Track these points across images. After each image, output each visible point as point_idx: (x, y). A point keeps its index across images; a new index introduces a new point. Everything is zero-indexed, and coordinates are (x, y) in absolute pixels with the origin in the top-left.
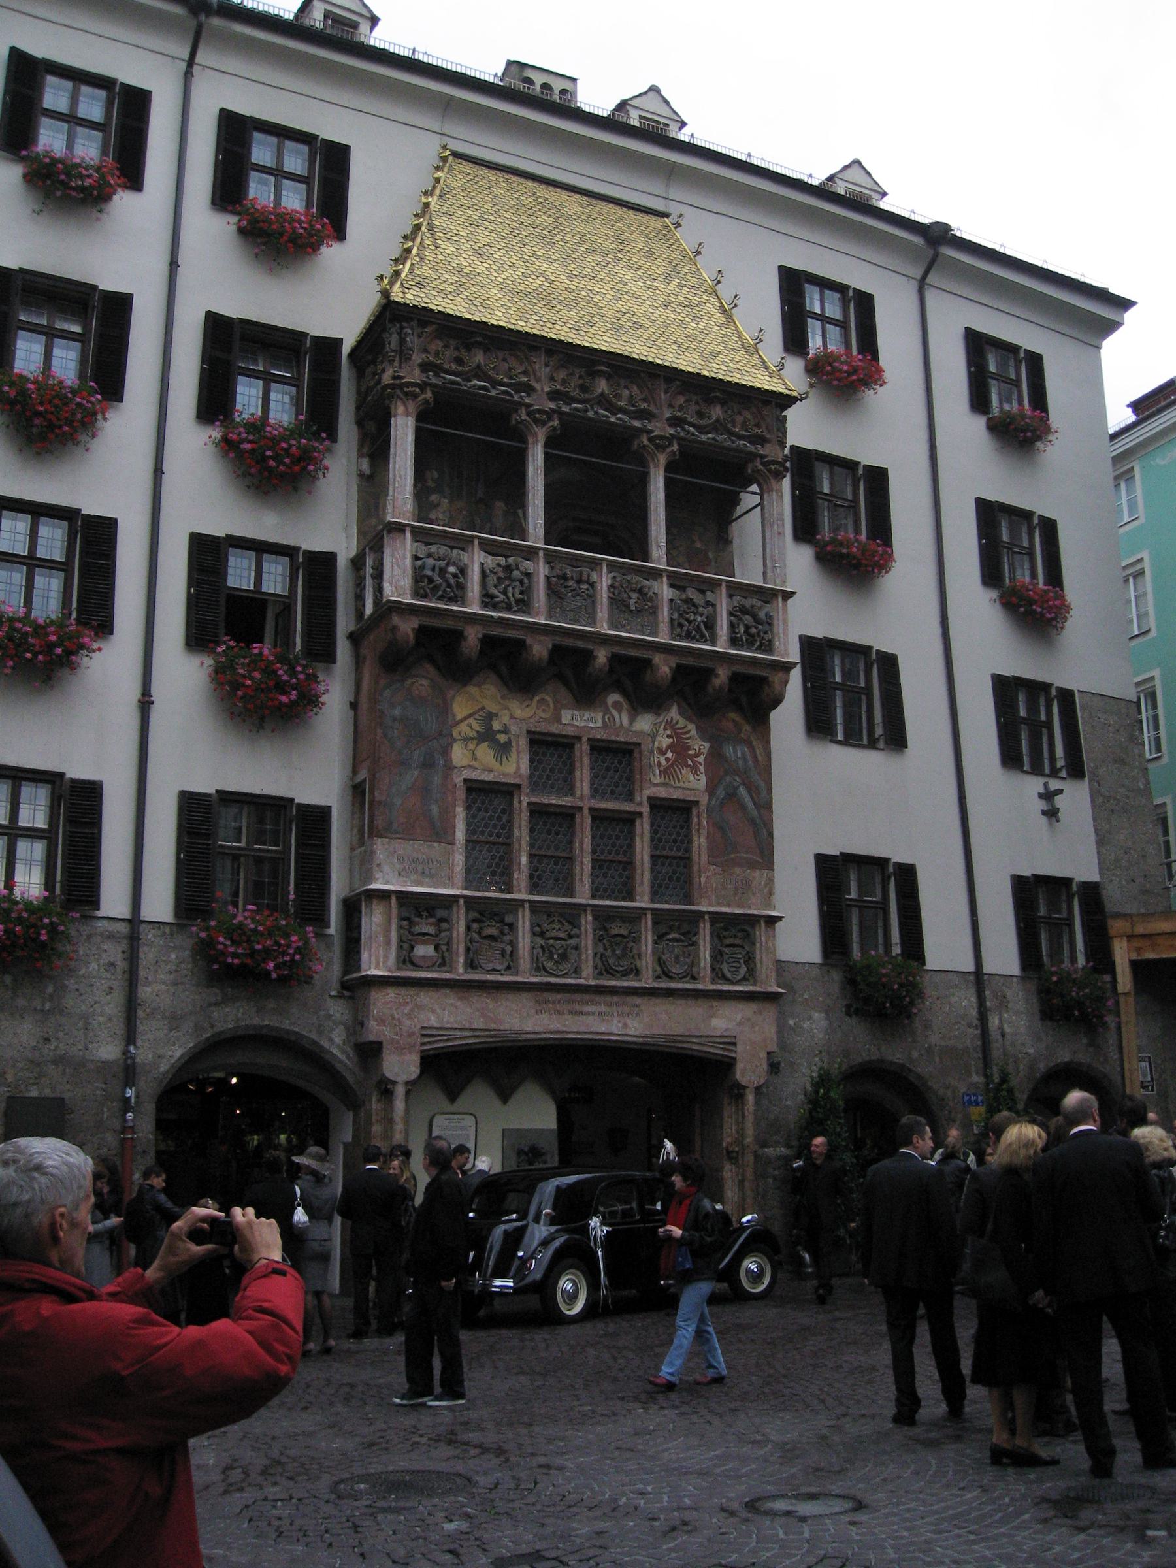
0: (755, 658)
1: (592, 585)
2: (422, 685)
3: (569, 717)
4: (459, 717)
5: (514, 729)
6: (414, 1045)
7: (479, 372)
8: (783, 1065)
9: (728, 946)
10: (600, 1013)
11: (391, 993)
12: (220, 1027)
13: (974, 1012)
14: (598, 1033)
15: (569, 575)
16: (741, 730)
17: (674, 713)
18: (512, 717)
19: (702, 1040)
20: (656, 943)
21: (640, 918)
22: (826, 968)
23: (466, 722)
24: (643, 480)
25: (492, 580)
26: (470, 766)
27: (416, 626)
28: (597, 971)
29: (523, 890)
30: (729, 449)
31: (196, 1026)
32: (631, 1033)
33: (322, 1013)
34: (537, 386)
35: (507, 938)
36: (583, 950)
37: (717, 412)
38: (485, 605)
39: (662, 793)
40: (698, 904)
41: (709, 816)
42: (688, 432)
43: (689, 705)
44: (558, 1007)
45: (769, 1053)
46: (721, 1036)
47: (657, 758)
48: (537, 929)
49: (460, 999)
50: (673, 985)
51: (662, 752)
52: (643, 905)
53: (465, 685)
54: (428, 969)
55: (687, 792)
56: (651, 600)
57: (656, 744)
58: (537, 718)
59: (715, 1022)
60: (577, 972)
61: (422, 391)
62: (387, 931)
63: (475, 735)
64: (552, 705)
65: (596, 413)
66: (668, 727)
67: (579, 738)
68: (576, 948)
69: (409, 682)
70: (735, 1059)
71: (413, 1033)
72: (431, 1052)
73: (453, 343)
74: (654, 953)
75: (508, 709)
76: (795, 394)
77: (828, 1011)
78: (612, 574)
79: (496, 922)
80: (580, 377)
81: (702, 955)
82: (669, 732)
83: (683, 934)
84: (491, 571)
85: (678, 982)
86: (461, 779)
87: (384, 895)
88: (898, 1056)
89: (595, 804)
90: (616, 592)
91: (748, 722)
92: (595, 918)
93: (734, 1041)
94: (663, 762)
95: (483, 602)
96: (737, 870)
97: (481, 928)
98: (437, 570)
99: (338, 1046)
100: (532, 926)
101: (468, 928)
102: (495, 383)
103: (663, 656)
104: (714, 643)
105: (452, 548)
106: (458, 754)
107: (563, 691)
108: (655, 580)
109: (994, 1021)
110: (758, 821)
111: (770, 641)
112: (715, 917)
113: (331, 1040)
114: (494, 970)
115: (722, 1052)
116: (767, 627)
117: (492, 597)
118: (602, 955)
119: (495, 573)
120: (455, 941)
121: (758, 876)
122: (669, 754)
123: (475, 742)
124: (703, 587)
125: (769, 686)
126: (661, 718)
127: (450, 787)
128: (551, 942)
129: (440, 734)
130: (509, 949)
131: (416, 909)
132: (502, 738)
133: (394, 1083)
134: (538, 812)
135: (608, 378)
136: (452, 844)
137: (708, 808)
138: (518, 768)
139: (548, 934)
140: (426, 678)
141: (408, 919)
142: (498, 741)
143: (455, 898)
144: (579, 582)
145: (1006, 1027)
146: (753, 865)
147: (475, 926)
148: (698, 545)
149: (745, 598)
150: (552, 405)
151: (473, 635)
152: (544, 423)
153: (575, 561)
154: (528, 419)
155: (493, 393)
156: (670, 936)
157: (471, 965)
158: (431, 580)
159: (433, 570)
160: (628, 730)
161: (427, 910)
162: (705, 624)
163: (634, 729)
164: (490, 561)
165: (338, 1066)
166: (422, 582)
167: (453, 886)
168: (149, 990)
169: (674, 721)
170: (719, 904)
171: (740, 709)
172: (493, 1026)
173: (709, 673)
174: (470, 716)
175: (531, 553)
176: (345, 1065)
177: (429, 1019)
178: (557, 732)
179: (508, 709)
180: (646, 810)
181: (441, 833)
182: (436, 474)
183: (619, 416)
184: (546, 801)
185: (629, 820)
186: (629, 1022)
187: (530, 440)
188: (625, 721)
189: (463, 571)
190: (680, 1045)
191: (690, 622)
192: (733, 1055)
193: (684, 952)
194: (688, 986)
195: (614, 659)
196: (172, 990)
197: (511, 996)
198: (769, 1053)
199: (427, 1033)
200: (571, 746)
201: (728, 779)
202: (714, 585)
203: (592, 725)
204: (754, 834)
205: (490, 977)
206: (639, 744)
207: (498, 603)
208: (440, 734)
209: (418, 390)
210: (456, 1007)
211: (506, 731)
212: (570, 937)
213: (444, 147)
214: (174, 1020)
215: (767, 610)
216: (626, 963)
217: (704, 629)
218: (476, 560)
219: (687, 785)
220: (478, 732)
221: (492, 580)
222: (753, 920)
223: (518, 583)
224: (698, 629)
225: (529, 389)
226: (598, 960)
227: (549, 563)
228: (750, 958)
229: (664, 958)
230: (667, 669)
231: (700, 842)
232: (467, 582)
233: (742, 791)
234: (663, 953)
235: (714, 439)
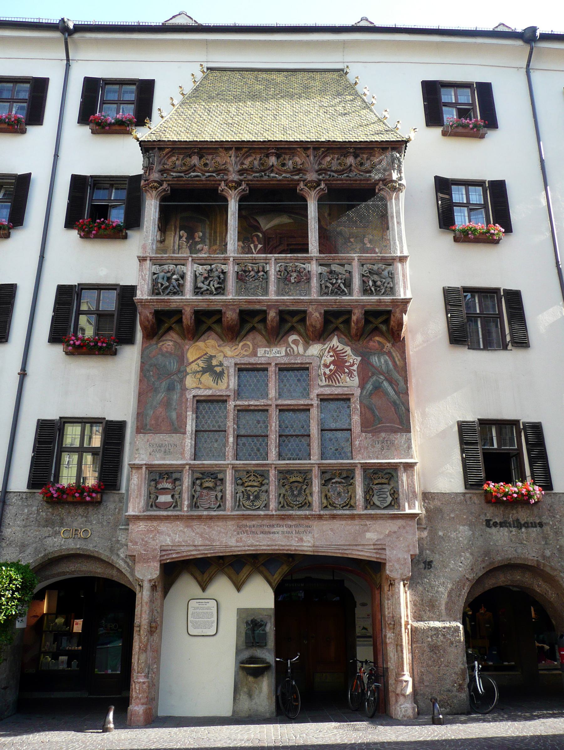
0: (380, 300)
1: (266, 273)
2: (169, 345)
3: (263, 352)
4: (191, 361)
5: (226, 363)
6: (154, 557)
7: (193, 168)
8: (434, 563)
9: (377, 484)
10: (283, 532)
11: (142, 526)
12: (50, 550)
14: (282, 546)
15: (251, 269)
16: (384, 346)
17: (335, 342)
18: (225, 356)
19: (360, 548)
20: (324, 485)
21: (311, 470)
22: (467, 496)
23: (196, 362)
24: (305, 208)
25: (200, 279)
26: (197, 388)
27: (153, 311)
28: (280, 506)
29: (230, 458)
30: (361, 180)
31: (36, 549)
32: (305, 544)
33: (114, 539)
34: (231, 169)
35: (218, 488)
36: (271, 493)
38: (196, 293)
39: (327, 391)
40: (355, 459)
42: (330, 175)
43: (346, 336)
44: (253, 529)
45: (411, 555)
46: (374, 545)
47: (323, 370)
48: (239, 481)
49: (187, 527)
50: (335, 512)
51: (326, 366)
52: (312, 462)
53: (197, 341)
54: (166, 509)
55: (346, 389)
56: (306, 275)
57: (323, 362)
58: (242, 355)
59: (369, 535)
60: (266, 506)
61: (161, 185)
62: (139, 489)
63: (201, 369)
64: (251, 347)
65: (268, 176)
66: (330, 350)
67: (270, 364)
68: (267, 491)
69: (161, 344)
70: (386, 559)
71: (156, 549)
72: (168, 561)
73: (182, 156)
74: (321, 492)
75: (222, 352)
76: (404, 139)
77: (471, 525)
78: (280, 265)
79: (212, 478)
80: (260, 159)
81: (357, 490)
82: (331, 354)
83: (343, 478)
84: (200, 274)
85: (340, 509)
86: (192, 395)
87: (138, 467)
88: (534, 555)
89: (280, 402)
90: (282, 275)
91: (389, 342)
92: (280, 472)
93: (384, 547)
94: (328, 372)
95: (195, 292)
96: (383, 435)
97: (201, 485)
98: (165, 279)
99: (122, 559)
100: (236, 479)
101: (194, 484)
103: (314, 307)
104: (350, 294)
105: (176, 265)
106: (190, 381)
107: (259, 338)
108: (309, 263)
110: (398, 402)
111: (392, 288)
112: (365, 467)
113: (118, 555)
114: (209, 508)
115: (375, 555)
116: (389, 280)
117: (201, 288)
118: (284, 495)
119: (202, 275)
120: (184, 491)
121: (400, 438)
122: (332, 367)
123: (201, 373)
124: (344, 262)
125: (394, 316)
126: (326, 346)
127: (184, 400)
128: (248, 488)
129: (179, 371)
130: (220, 495)
131: (160, 474)
132: (218, 369)
133: (142, 581)
134: (241, 410)
135: (278, 156)
136: (185, 433)
137: (360, 397)
138: (228, 385)
139: (246, 484)
140: (171, 341)
141: (154, 480)
142: (215, 372)
143: (183, 466)
144: (259, 272)
147: (198, 482)
148: (368, 245)
149: (374, 265)
150: (241, 178)
152: (236, 188)
153: (254, 261)
154: (226, 188)
155: (203, 178)
156: (334, 481)
157: (194, 505)
158: (162, 285)
159: (163, 279)
160: (303, 355)
161: (166, 474)
162: (344, 284)
163: (306, 354)
164: (201, 269)
165: (123, 570)
167: (183, 458)
168: (10, 530)
169: (335, 347)
170: (370, 458)
171: (382, 334)
172: (208, 543)
173: (349, 313)
174: (199, 358)
176: (127, 570)
177: (166, 540)
178: (254, 362)
179: (222, 352)
180: (315, 402)
182: (201, 234)
183: (283, 175)
184: (246, 403)
185: (306, 409)
186: (304, 538)
187: (229, 199)
188: (301, 349)
189: (183, 277)
190: (343, 552)
191: (333, 284)
192: (383, 557)
193: (344, 490)
194: (347, 512)
196: (23, 530)
197: (220, 523)
198: (411, 555)
200: (266, 370)
201: (375, 378)
203: (278, 355)
204: (395, 410)
205: (205, 513)
206: (311, 363)
207: (205, 291)
208: (179, 371)
209: (156, 184)
210: (184, 532)
212: (262, 485)
214: (23, 547)
215: (389, 269)
216: (301, 499)
217: (343, 288)
218: (189, 270)
219: (345, 384)
220: (202, 367)
221: (200, 279)
222: (395, 467)
223: (217, 278)
225: (225, 171)
226: (281, 500)
227: (238, 264)
228: (394, 491)
229: (329, 494)
230: (317, 314)
232: (184, 282)
234: (329, 491)
235: (347, 176)
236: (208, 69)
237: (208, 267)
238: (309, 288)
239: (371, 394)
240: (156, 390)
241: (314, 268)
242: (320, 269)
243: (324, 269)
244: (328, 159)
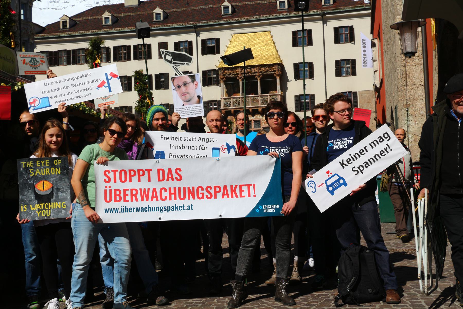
34: (239, 73)
37: (267, 69)
39: (264, 126)
51: (264, 120)
61: (223, 79)
94: (264, 122)
102: (233, 75)
135: (250, 69)
151: (232, 110)
155: (233, 76)
164: (234, 100)
166: (225, 105)
175: (239, 98)
189: (231, 102)
195: (253, 110)
202: (267, 96)
213: (231, 34)
221: (234, 103)
224: (265, 103)
225: (238, 74)
236: (233, 34)
237: (236, 100)
238: (258, 103)
241: (259, 98)
242: (261, 98)
243: (262, 98)
244: (262, 68)
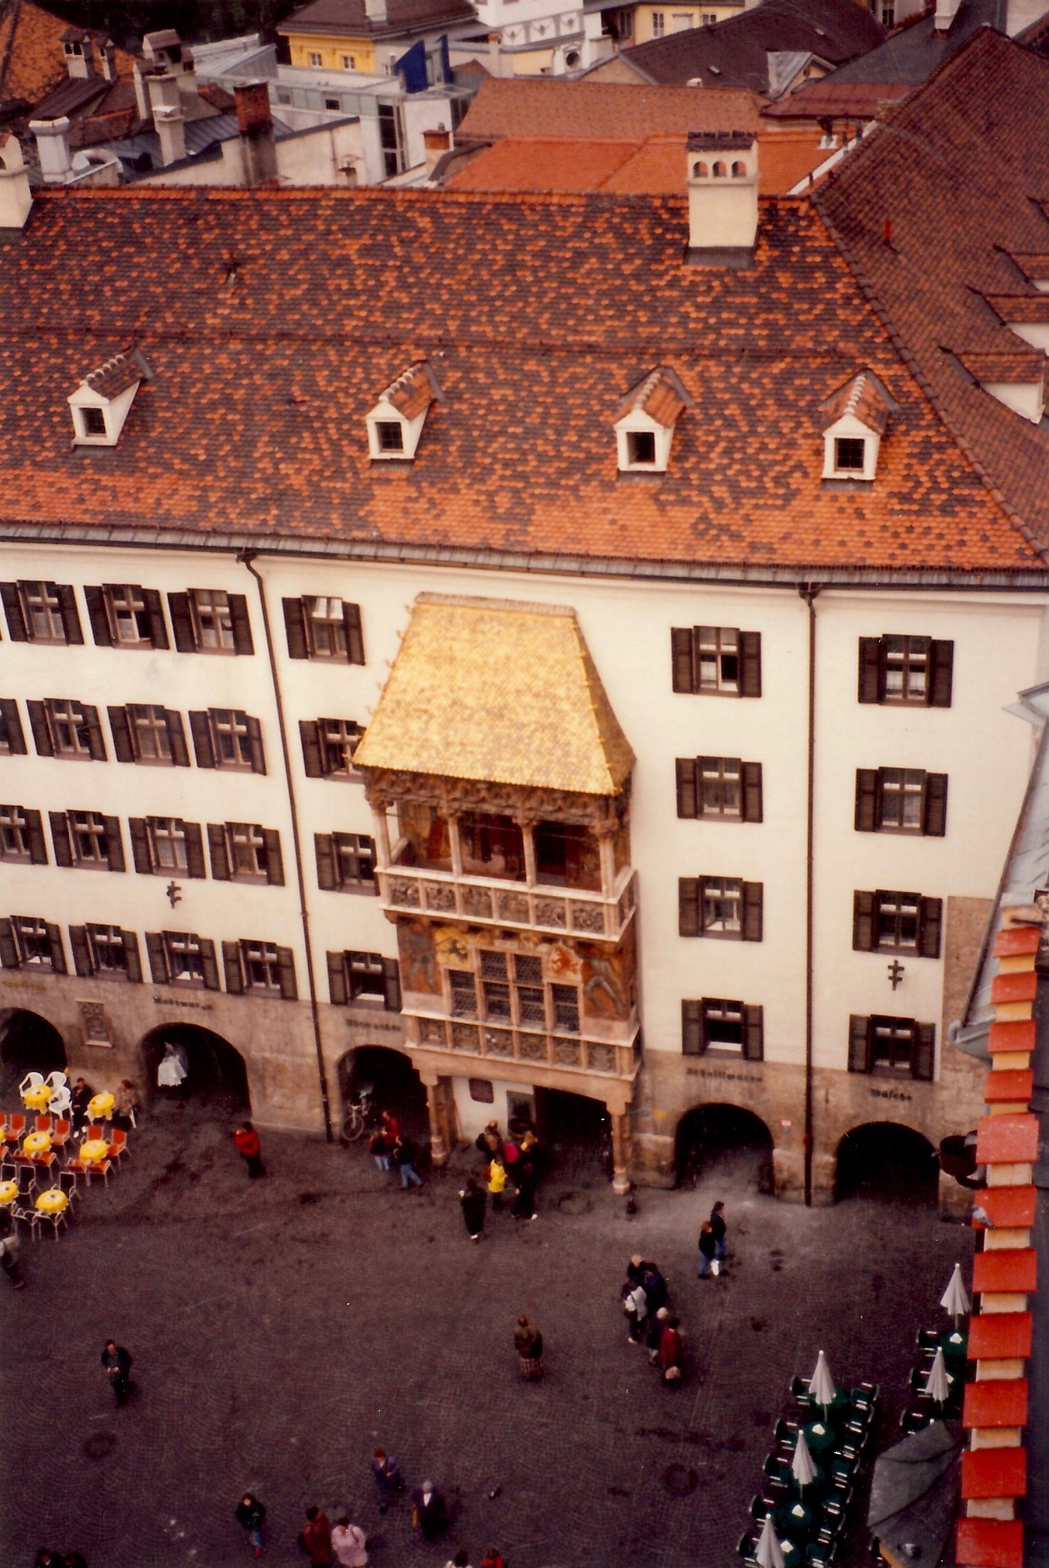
13: (803, 1087)
39: (556, 981)
41: (585, 993)
47: (551, 965)
106: (441, 958)
109: (819, 1095)
112: (589, 1043)
145: (831, 1098)
146: (613, 1019)
181: (436, 990)
189: (417, 891)
199: (437, 1069)
201: (595, 978)
211: (464, 948)
222: (614, 1046)
231: (581, 1005)
233: (605, 984)
239: (592, 990)
240: (414, 960)
